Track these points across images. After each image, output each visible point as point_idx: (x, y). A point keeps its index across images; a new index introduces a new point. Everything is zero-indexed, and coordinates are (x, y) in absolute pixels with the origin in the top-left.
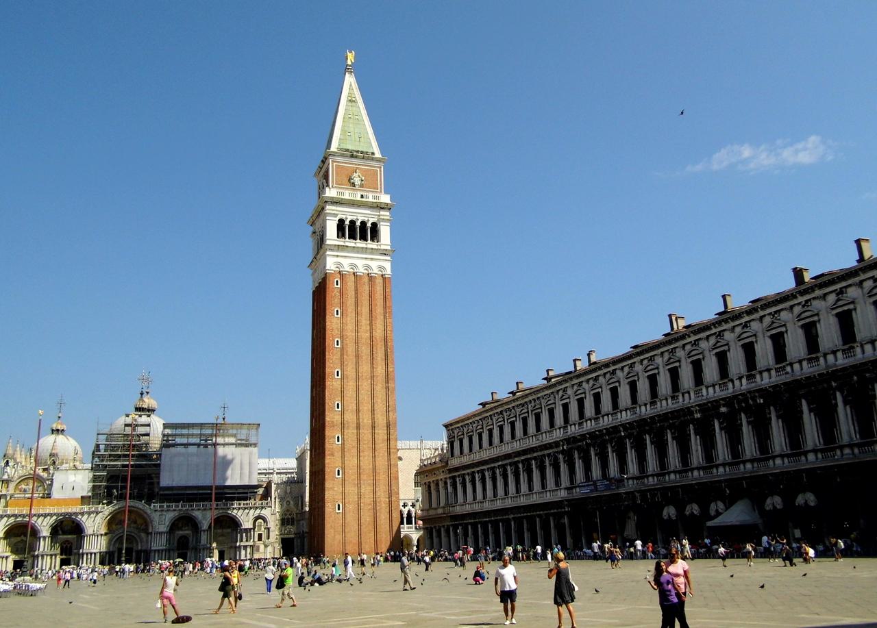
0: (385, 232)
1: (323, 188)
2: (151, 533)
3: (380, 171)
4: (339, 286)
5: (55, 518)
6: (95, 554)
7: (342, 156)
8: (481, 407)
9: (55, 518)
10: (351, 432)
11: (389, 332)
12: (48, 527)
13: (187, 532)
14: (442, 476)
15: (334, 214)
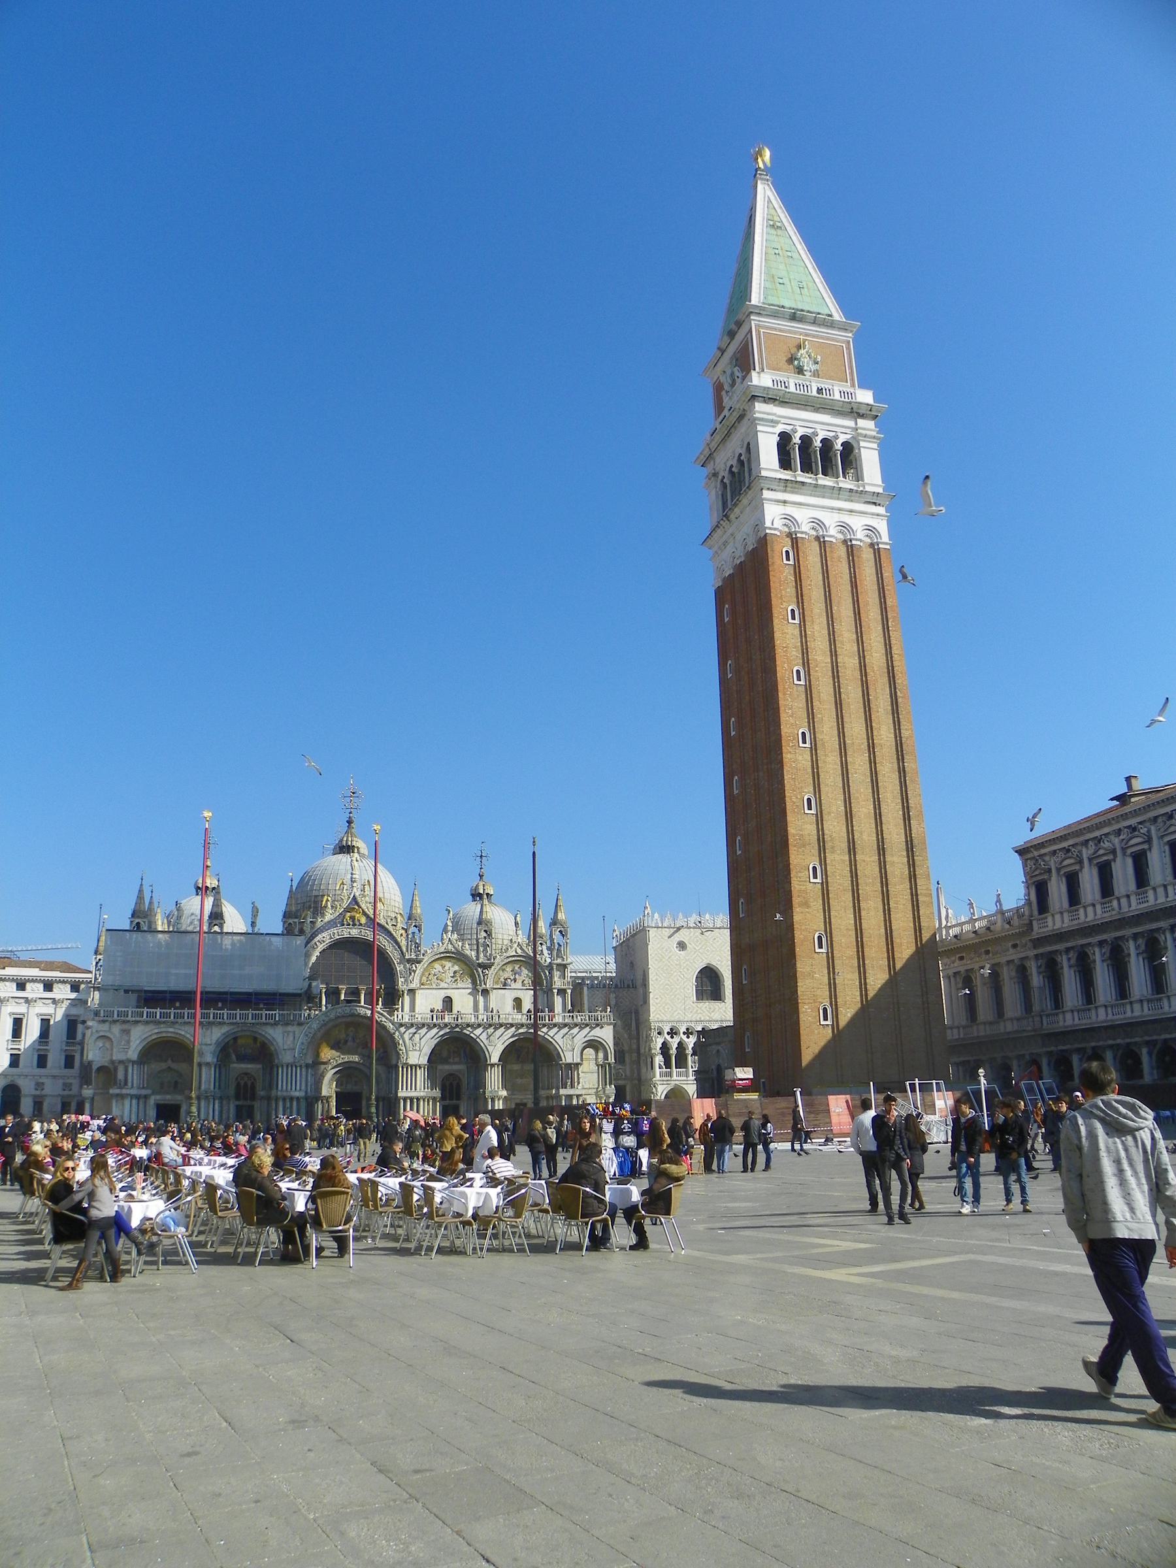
0: (870, 458)
1: (733, 384)
2: (397, 1067)
3: (848, 348)
4: (791, 562)
5: (225, 1029)
6: (298, 1099)
7: (775, 315)
8: (1116, 803)
9: (225, 1029)
10: (838, 859)
11: (895, 657)
12: (212, 1048)
13: (455, 1067)
14: (1013, 955)
15: (772, 421)
